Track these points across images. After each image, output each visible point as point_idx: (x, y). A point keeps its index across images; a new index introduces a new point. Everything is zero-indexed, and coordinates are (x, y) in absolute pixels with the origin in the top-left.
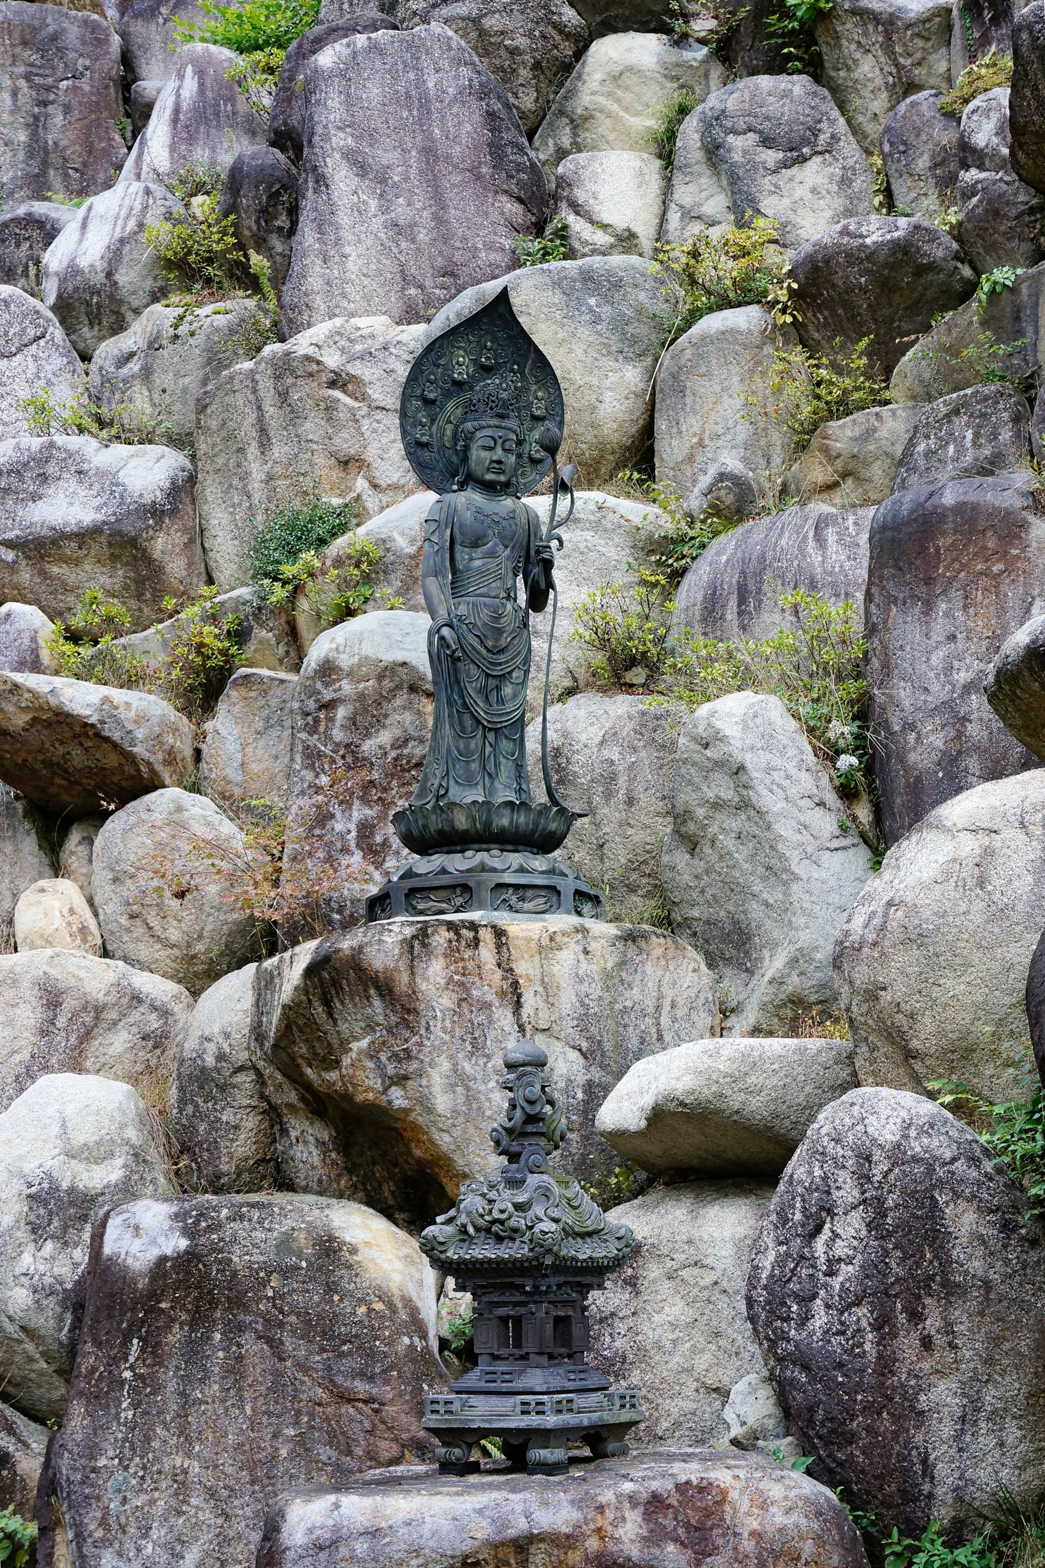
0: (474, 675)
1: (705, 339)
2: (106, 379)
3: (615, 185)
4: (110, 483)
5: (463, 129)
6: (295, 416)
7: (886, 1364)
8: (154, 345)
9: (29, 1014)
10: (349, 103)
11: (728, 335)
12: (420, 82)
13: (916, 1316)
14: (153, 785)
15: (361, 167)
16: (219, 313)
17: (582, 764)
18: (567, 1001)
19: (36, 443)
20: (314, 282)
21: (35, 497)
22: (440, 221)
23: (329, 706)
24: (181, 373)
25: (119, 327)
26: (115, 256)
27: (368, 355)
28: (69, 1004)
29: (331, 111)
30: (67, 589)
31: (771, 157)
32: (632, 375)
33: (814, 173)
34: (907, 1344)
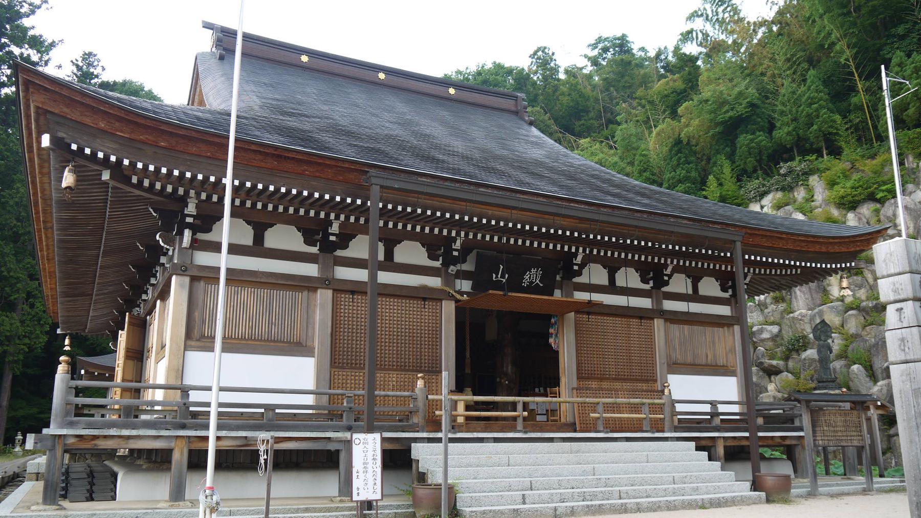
0: (824, 361)
4: (770, 331)
17: (838, 370)
24: (777, 316)
32: (840, 318)
33: (863, 291)
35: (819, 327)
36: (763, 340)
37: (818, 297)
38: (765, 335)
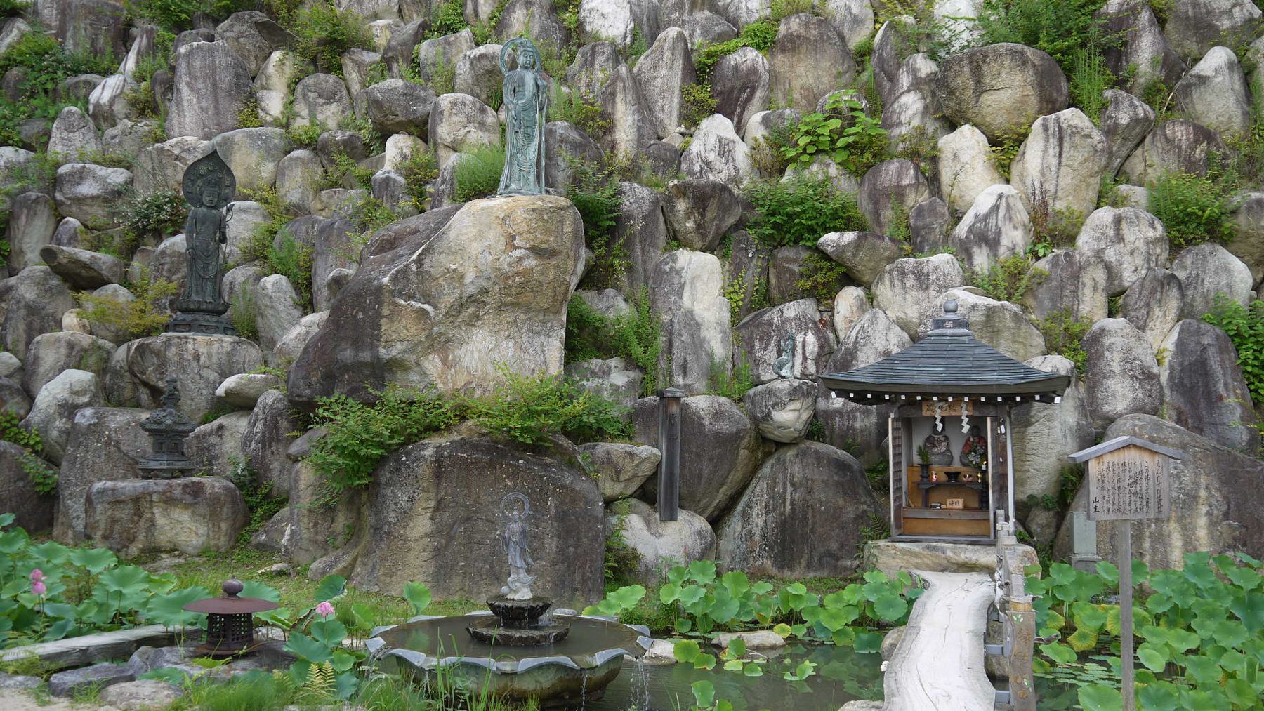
1: (291, 159)
2: (108, 144)
3: (273, 103)
5: (226, 78)
6: (164, 168)
7: (263, 457)
8: (124, 134)
9: (63, 351)
10: (189, 66)
11: (298, 159)
12: (213, 62)
13: (271, 447)
14: (109, 282)
15: (192, 89)
16: (144, 126)
18: (215, 359)
19: (80, 165)
20: (175, 122)
21: (78, 184)
22: (216, 108)
23: (163, 264)
25: (114, 125)
26: (113, 100)
27: (188, 151)
28: (76, 348)
29: (182, 68)
30: (88, 213)
31: (321, 101)
33: (334, 107)
34: (268, 453)
35: (203, 169)
36: (80, 200)
37: (232, 109)
38: (88, 188)
